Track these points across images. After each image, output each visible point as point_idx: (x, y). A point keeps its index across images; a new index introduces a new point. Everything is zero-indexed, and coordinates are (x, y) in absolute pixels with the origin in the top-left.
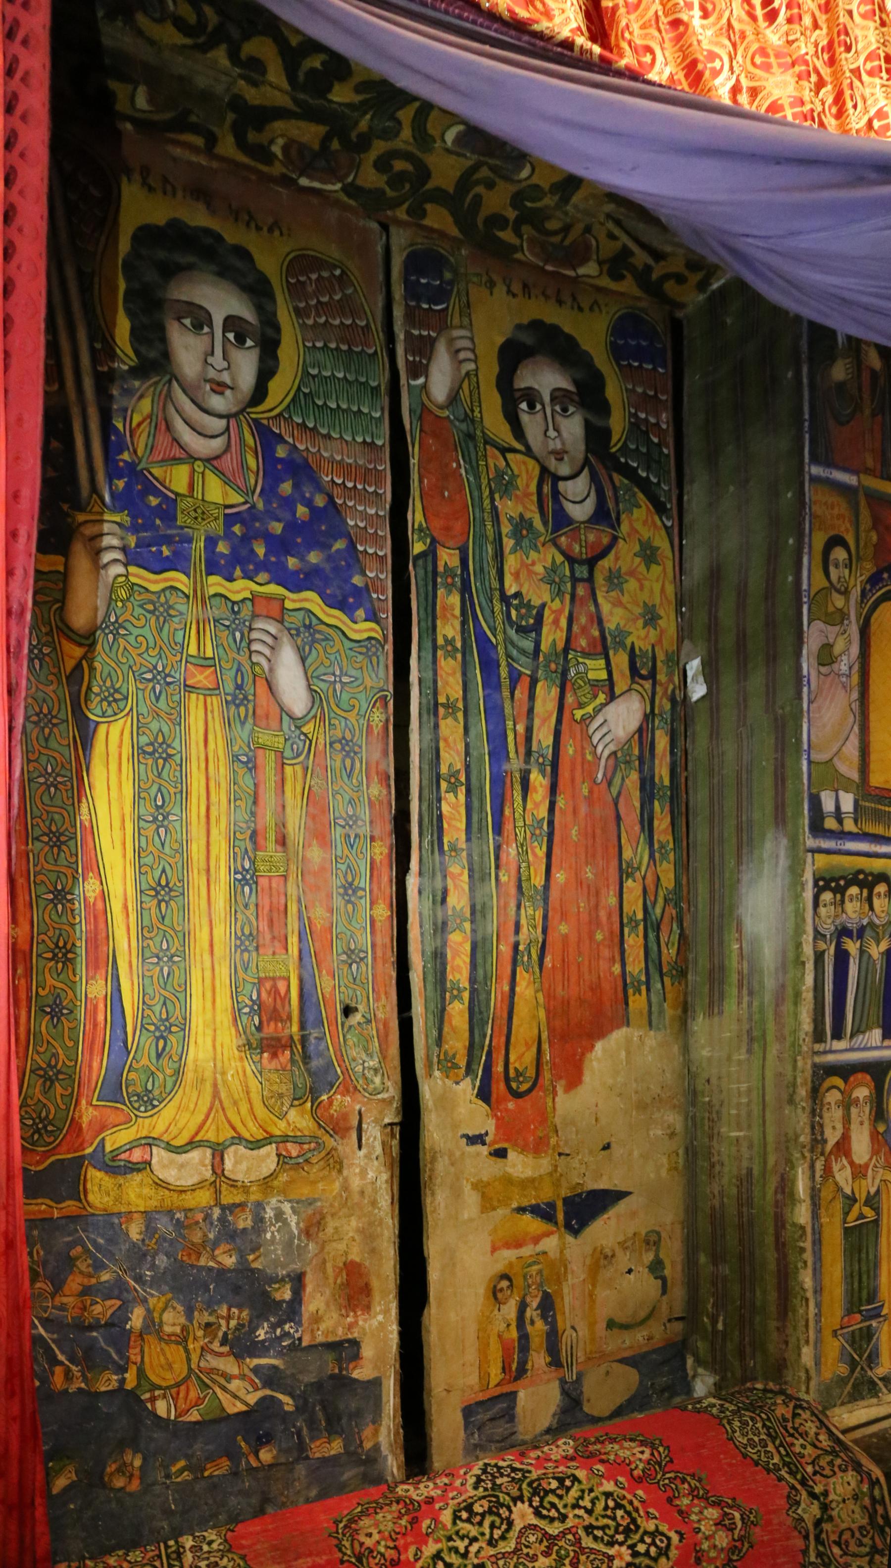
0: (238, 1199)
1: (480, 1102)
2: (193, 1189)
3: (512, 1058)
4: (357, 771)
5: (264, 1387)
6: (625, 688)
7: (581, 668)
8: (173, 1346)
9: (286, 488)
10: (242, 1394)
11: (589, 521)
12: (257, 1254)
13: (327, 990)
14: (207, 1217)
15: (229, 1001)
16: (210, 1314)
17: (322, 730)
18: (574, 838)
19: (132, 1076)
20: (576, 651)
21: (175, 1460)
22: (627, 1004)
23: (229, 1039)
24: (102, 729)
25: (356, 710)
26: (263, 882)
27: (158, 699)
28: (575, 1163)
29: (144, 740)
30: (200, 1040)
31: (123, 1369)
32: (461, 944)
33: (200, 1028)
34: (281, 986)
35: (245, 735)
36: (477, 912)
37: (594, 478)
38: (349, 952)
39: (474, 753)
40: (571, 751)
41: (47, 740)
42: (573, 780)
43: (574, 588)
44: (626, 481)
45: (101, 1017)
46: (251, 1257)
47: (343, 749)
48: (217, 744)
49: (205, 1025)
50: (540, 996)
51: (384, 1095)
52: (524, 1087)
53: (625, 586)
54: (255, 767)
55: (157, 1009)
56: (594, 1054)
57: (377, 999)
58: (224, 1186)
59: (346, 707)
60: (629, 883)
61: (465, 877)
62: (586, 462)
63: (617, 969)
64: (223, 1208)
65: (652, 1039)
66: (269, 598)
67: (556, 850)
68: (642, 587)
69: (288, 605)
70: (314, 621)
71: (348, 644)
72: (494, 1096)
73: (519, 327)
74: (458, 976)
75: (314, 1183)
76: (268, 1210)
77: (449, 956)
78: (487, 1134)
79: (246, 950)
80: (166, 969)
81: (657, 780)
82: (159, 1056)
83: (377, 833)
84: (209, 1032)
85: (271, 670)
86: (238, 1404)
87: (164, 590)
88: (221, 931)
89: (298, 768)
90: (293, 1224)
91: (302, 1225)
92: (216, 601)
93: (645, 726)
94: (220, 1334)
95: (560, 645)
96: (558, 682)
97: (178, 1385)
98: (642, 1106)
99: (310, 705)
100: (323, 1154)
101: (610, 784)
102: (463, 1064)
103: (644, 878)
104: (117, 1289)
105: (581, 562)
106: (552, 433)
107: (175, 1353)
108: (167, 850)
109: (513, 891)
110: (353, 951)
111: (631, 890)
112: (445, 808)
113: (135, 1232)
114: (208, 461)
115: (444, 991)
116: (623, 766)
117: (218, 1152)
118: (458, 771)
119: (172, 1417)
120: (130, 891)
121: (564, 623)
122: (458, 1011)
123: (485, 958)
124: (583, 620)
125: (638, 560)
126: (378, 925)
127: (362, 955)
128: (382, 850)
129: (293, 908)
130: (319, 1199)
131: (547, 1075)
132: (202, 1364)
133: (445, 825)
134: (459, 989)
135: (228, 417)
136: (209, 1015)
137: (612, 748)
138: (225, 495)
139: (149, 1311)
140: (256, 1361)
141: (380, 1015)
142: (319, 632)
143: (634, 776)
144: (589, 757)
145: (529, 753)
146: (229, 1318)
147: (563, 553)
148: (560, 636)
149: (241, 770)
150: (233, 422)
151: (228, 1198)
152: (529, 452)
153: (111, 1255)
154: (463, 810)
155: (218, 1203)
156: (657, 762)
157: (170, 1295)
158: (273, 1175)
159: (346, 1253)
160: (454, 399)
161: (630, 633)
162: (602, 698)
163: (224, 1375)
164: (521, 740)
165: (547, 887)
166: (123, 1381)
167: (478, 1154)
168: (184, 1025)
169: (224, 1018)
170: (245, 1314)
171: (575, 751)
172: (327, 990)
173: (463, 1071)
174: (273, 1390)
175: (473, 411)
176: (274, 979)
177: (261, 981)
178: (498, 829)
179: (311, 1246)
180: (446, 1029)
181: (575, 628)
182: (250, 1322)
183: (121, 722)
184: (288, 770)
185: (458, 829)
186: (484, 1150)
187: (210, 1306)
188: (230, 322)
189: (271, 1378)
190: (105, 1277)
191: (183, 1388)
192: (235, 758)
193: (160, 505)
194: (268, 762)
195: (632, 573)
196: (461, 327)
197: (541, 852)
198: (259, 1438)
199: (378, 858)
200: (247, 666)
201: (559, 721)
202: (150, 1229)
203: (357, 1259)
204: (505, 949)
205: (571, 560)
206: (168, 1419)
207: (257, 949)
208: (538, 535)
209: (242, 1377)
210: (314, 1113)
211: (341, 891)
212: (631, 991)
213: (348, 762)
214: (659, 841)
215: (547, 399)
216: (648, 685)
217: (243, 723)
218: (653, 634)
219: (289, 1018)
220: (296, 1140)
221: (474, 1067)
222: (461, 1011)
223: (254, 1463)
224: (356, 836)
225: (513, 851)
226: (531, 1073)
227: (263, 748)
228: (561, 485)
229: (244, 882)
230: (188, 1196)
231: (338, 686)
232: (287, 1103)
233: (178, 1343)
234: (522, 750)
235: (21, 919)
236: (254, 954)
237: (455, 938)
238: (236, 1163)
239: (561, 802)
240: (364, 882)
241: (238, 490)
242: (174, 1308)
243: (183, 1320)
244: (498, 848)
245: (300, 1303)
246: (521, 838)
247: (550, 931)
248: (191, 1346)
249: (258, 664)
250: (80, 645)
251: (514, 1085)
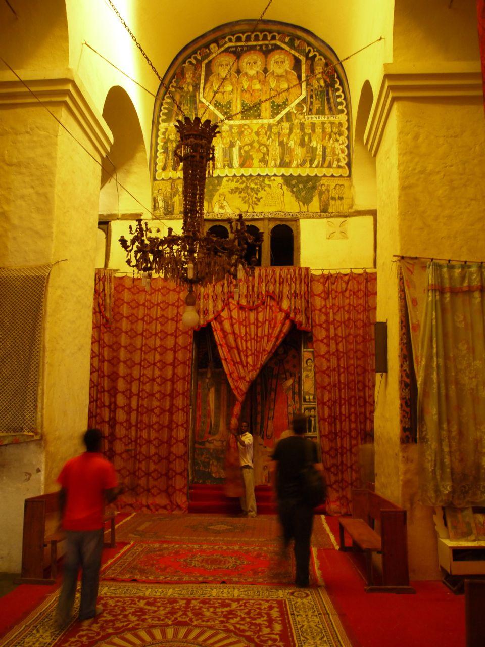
60: (289, 408)
113: (211, 451)
202: (213, 451)
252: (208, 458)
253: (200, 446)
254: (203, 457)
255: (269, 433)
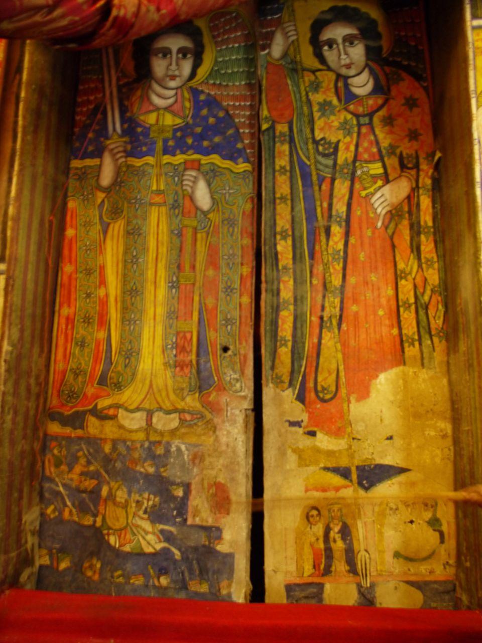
0: (158, 439)
1: (298, 403)
2: (136, 431)
3: (320, 379)
4: (235, 233)
5: (164, 541)
6: (396, 176)
7: (365, 169)
8: (120, 509)
9: (205, 112)
10: (153, 542)
11: (370, 94)
12: (166, 468)
13: (213, 338)
14: (142, 446)
15: (161, 342)
16: (139, 496)
17: (218, 215)
18: (362, 259)
19: (113, 375)
20: (360, 161)
21: (116, 570)
22: (403, 352)
23: (159, 360)
24: (111, 226)
25: (237, 204)
26: (183, 287)
27: (137, 210)
28: (366, 445)
29: (129, 228)
30: (146, 361)
31: (95, 516)
32: (287, 317)
33: (147, 354)
34: (188, 336)
35: (177, 221)
36: (298, 300)
37: (372, 72)
38: (227, 320)
39: (297, 219)
40: (359, 213)
41: (88, 232)
42: (361, 228)
43: (359, 129)
44: (394, 69)
45: (101, 348)
46: (162, 470)
47: (228, 223)
48: (164, 227)
49: (149, 353)
50: (339, 346)
51: (243, 394)
52: (328, 397)
53: (395, 123)
54: (181, 235)
55: (127, 344)
56: (378, 381)
57: (240, 343)
58: (151, 432)
59: (231, 204)
60: (403, 282)
61: (291, 282)
62: (367, 65)
63: (395, 331)
64: (150, 443)
65: (424, 374)
66: (193, 161)
67: (350, 267)
68: (407, 122)
69: (203, 162)
70: (216, 167)
71: (233, 175)
72: (307, 400)
73: (323, 12)
74: (284, 334)
75: (199, 436)
76: (173, 446)
77: (280, 322)
78: (302, 421)
79: (171, 318)
80: (132, 327)
81: (422, 223)
82: (126, 366)
83: (244, 262)
84: (150, 356)
85: (193, 192)
86: (150, 548)
87: (143, 165)
88: (160, 310)
89: (204, 235)
90: (186, 457)
91: (190, 457)
92: (167, 166)
93: (412, 195)
94: (144, 508)
95: (350, 160)
96: (349, 178)
97: (121, 530)
98: (417, 416)
99: (212, 205)
100: (205, 421)
101: (386, 228)
102: (287, 381)
103: (414, 279)
104: (96, 475)
105: (364, 116)
106: (343, 57)
107: (121, 512)
108: (137, 274)
109: (321, 288)
110: (229, 320)
111: (404, 286)
112: (279, 248)
113: (107, 448)
114: (168, 109)
115: (276, 341)
116: (396, 218)
117: (150, 414)
118: (287, 230)
119: (117, 546)
120: (119, 292)
121: (352, 148)
122: (285, 353)
123: (302, 326)
124: (366, 144)
125: (403, 108)
126: (243, 306)
127: (234, 321)
128: (247, 270)
129: (196, 298)
130: (201, 445)
131: (343, 391)
132: (134, 521)
133: (280, 257)
134: (285, 340)
135: (177, 88)
136: (151, 347)
137: (388, 208)
138: (174, 121)
139: (110, 489)
140: (161, 527)
141: (242, 352)
142: (218, 172)
143: (406, 222)
144: (372, 215)
145: (330, 216)
146: (148, 500)
147: (352, 113)
148: (350, 155)
149: (175, 238)
150: (179, 91)
151: (153, 438)
152: (329, 69)
153: (96, 459)
154: (290, 249)
155: (148, 439)
156: (422, 213)
157: (121, 482)
158: (177, 429)
159: (216, 477)
160: (285, 55)
161: (398, 147)
162: (380, 183)
163: (144, 530)
164: (326, 210)
165: (343, 286)
166: (95, 522)
167: (297, 432)
168: (138, 352)
169: (158, 351)
170: (157, 499)
171: (362, 212)
172: (213, 338)
173: (286, 385)
174: (170, 544)
175: (295, 57)
176: (185, 332)
177: (178, 333)
178: (312, 256)
179: (195, 470)
180: (277, 361)
181: (360, 149)
182: (160, 504)
183: (119, 222)
184: (199, 236)
185: (287, 258)
186: (301, 431)
187: (140, 492)
188: (180, 50)
189: (168, 537)
190: (92, 468)
191: (123, 532)
192: (172, 232)
193: (142, 131)
194: (189, 233)
195: (399, 115)
196: (289, 21)
197: (339, 267)
198: (160, 570)
199: (245, 274)
200: (180, 192)
201: (351, 198)
202: (114, 448)
203: (223, 482)
204: (315, 319)
205: (357, 116)
206: (115, 547)
207: (177, 318)
208: (335, 107)
209: (154, 533)
210: (200, 399)
211: (224, 290)
212: (406, 345)
213: (231, 229)
214: (425, 258)
215: (340, 41)
216: (413, 172)
217: (177, 216)
218: (416, 145)
219: (191, 351)
220: (189, 412)
221: (294, 383)
222: (286, 353)
223: (157, 584)
224: (233, 264)
225: (321, 268)
226: (333, 388)
227: (186, 226)
228: (350, 81)
229: (173, 287)
230: (134, 434)
231: (227, 195)
232: (186, 392)
233: (123, 508)
234: (326, 215)
235: (71, 305)
236: (175, 321)
237: (284, 313)
238: (158, 421)
239: (352, 240)
240: (237, 285)
241: (181, 117)
242: (122, 490)
243: (126, 496)
244: (311, 267)
245: (188, 499)
246: (325, 261)
247: (345, 310)
248: (129, 511)
249: (186, 190)
250: (104, 192)
251: (321, 395)
252: (96, 475)
253: (68, 430)
254: (78, 469)
255: (326, 379)
